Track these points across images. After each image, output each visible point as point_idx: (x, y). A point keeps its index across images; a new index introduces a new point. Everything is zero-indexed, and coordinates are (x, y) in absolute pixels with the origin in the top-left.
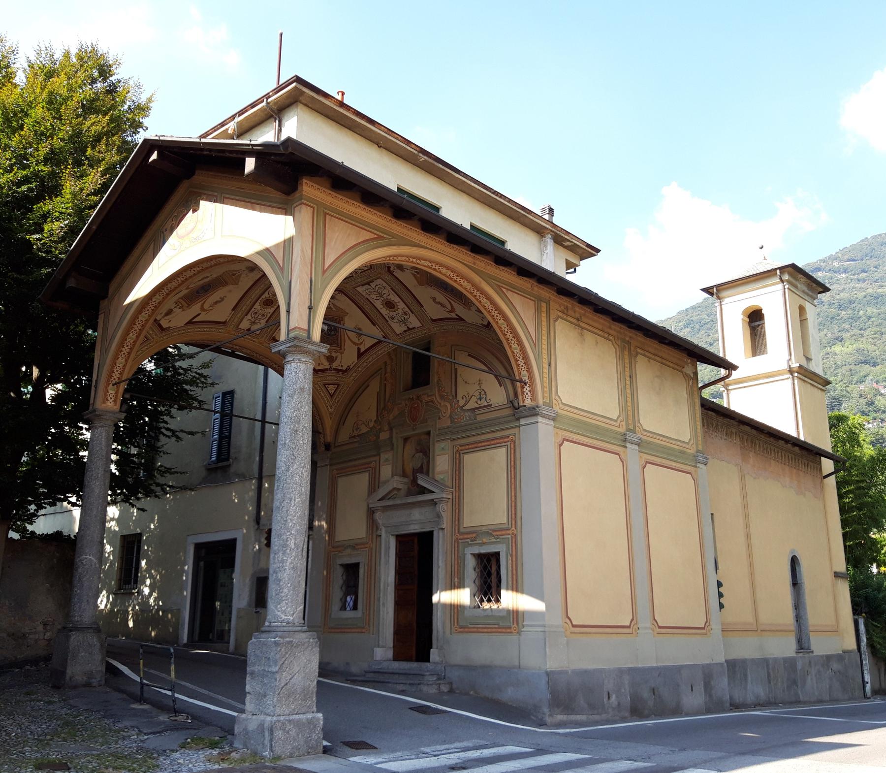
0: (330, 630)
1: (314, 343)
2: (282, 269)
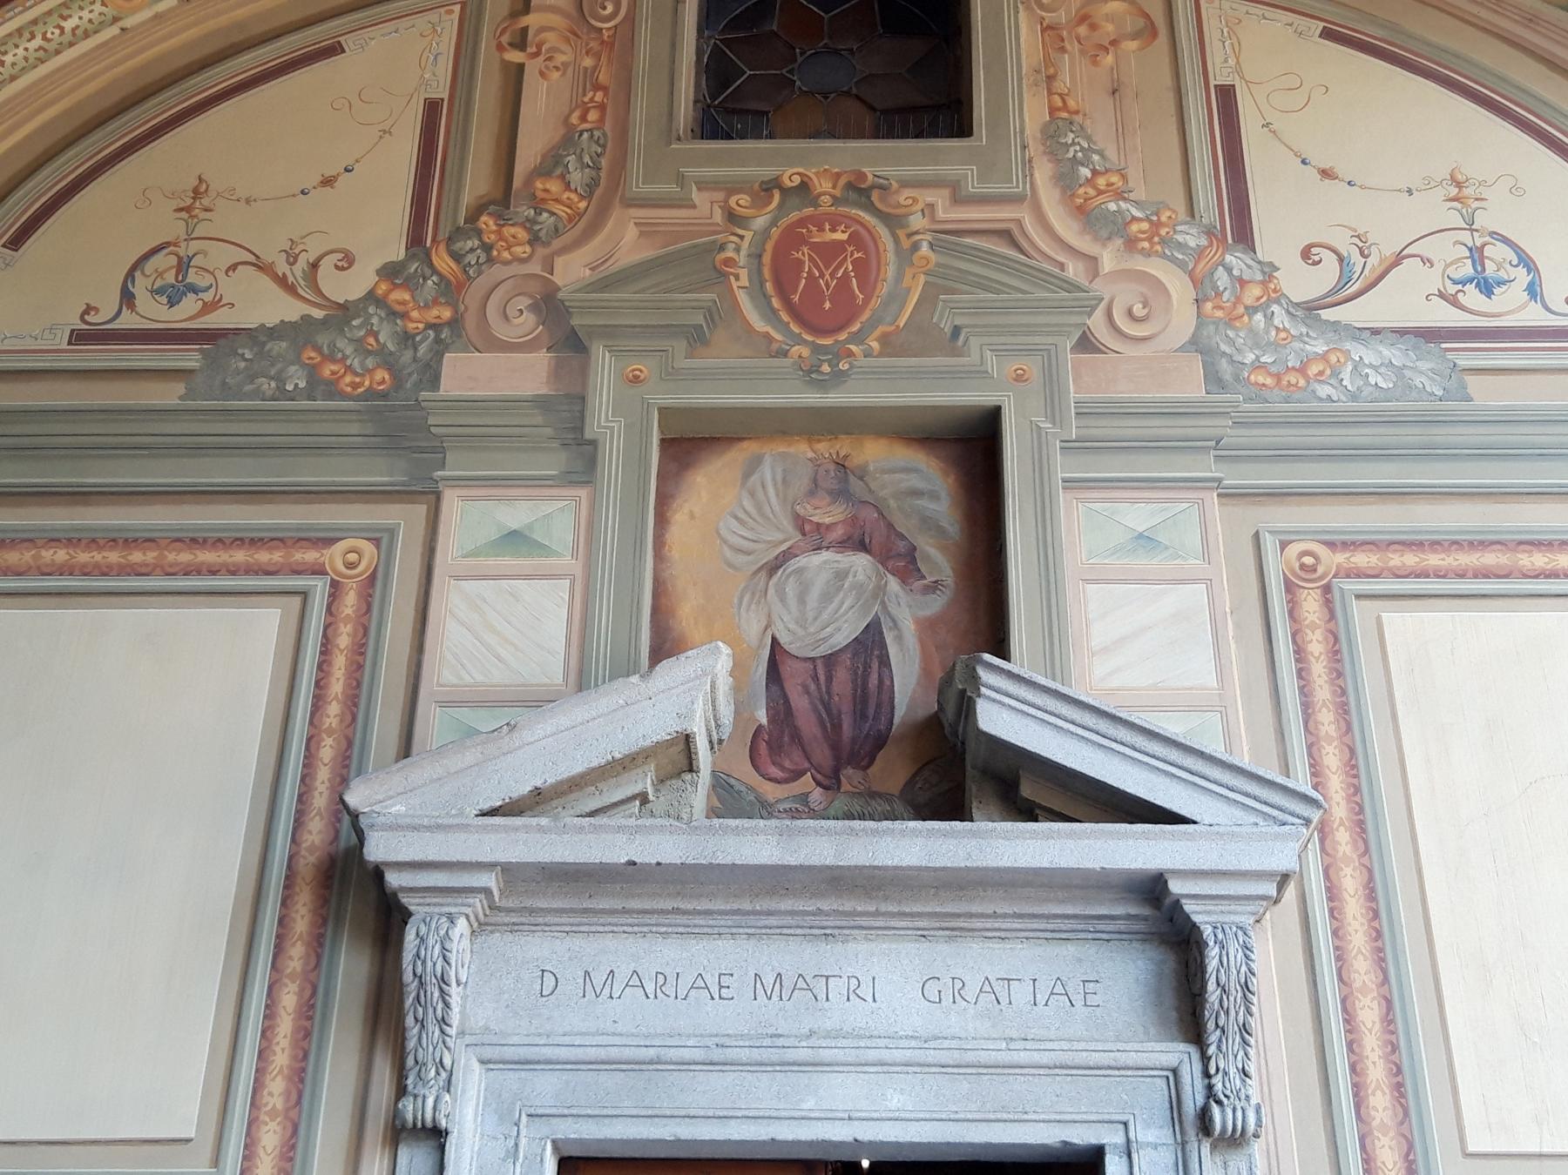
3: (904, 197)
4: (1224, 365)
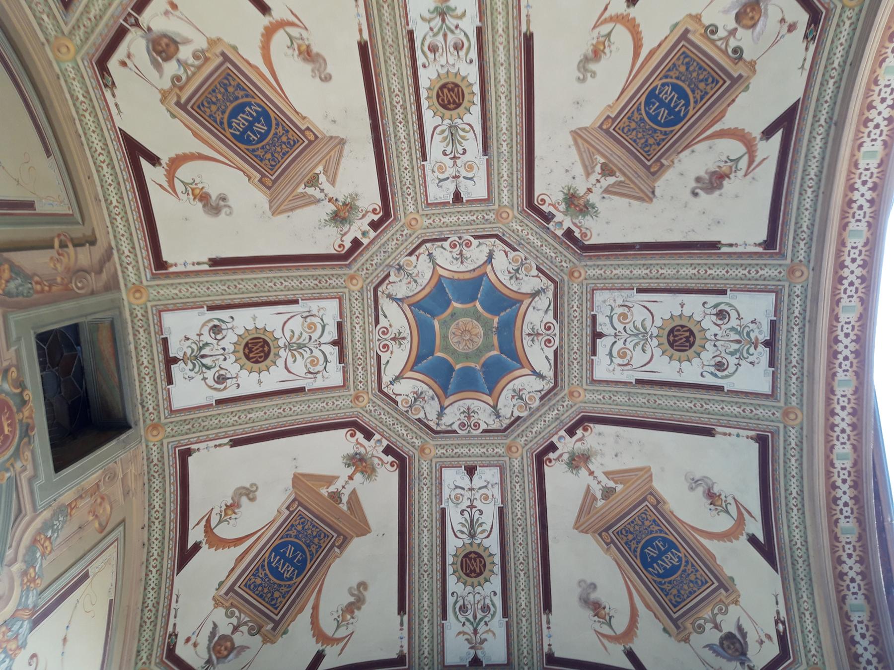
3: (28, 454)
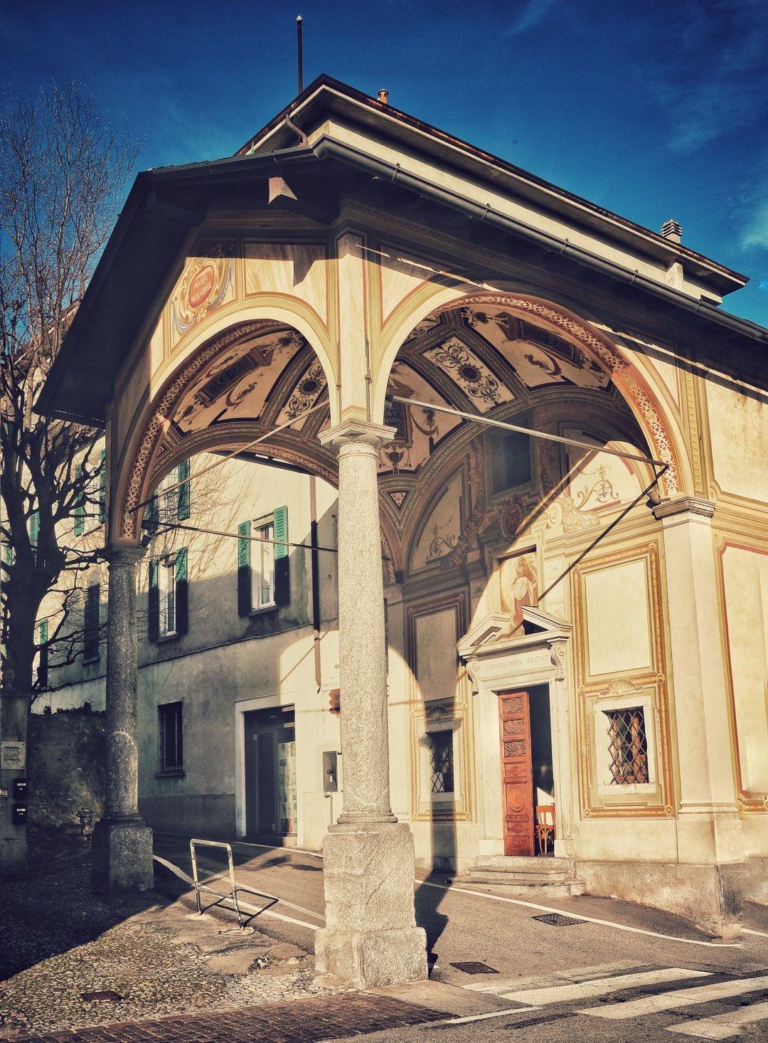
0: (420, 818)
1: (375, 427)
2: (326, 328)
4: (566, 527)
